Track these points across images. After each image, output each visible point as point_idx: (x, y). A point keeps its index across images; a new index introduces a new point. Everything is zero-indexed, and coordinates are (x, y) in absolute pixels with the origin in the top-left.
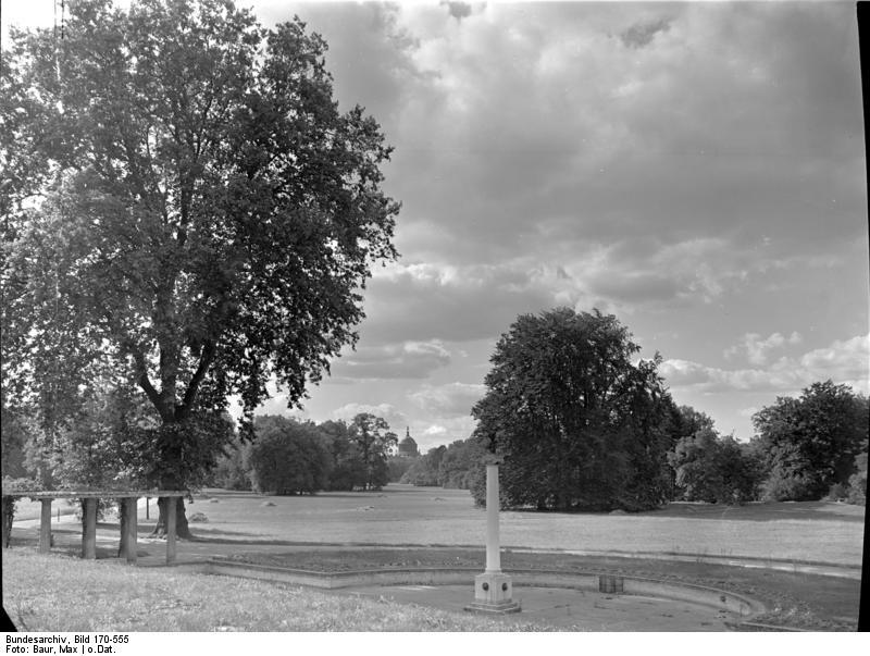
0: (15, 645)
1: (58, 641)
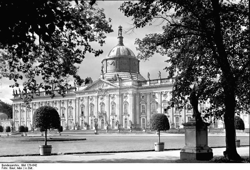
0: (4, 167)
1: (17, 166)
